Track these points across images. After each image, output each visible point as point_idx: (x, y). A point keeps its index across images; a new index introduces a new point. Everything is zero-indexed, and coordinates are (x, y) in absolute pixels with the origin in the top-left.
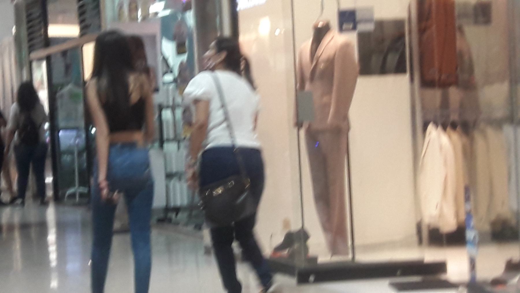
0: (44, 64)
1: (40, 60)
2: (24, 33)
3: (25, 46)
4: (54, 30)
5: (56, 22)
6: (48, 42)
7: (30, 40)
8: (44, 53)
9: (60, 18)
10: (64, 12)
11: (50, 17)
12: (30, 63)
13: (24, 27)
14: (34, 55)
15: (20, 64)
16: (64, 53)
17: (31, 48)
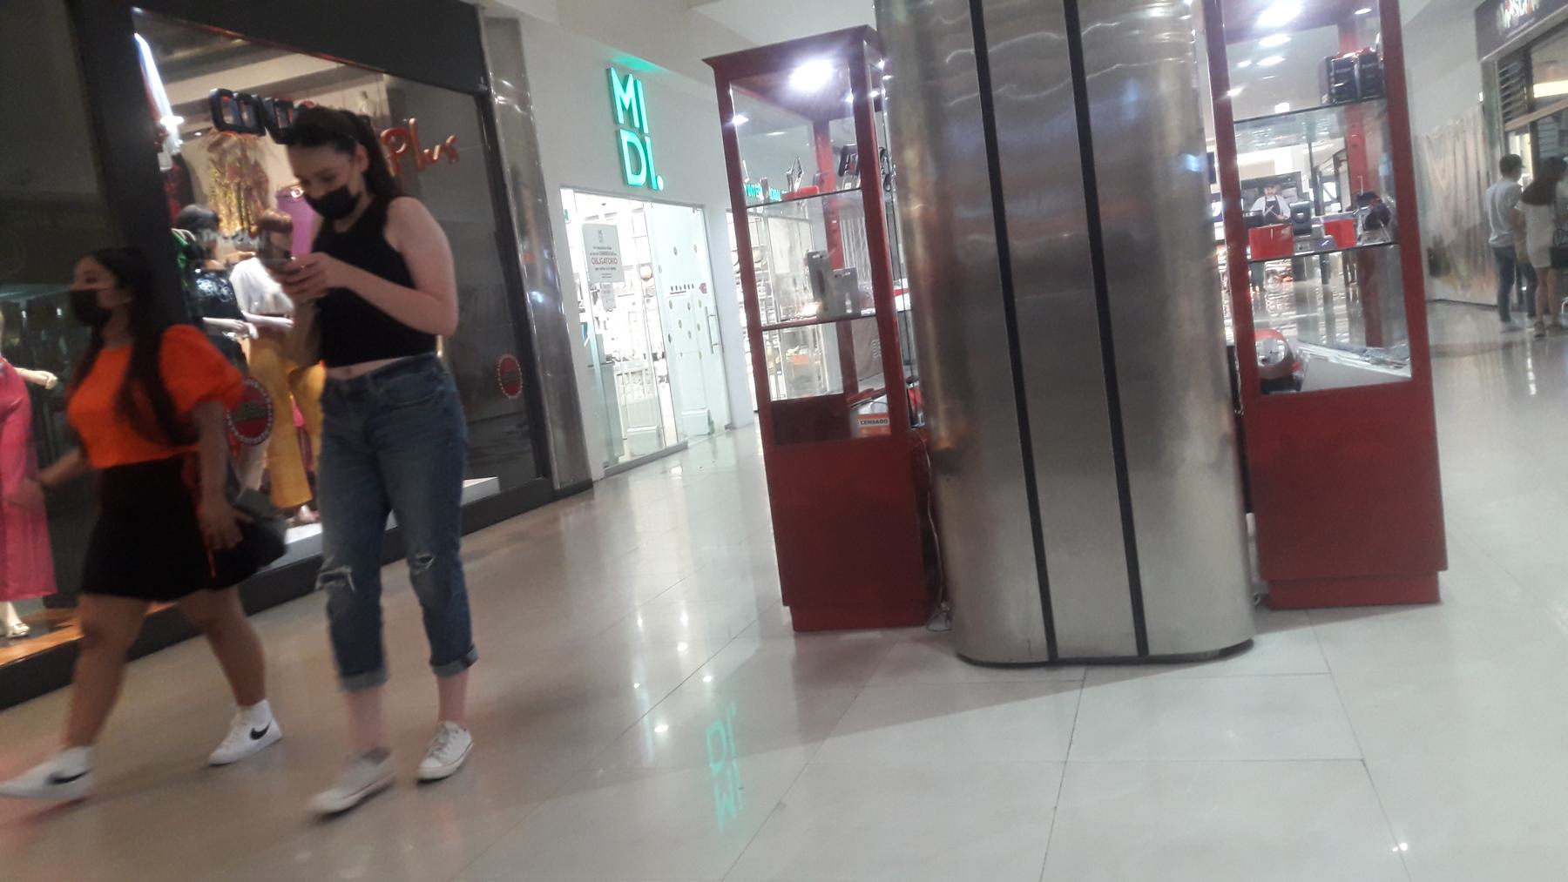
0: (1527, 137)
1: (1520, 131)
2: (1497, 96)
3: (1499, 114)
4: (1541, 90)
5: (1544, 79)
6: (1533, 105)
7: (1504, 107)
8: (1524, 120)
9: (1551, 68)
10: (1554, 62)
11: (1535, 71)
12: (1506, 134)
13: (1498, 89)
14: (1510, 125)
15: (1490, 141)
16: (1557, 117)
17: (1507, 117)
